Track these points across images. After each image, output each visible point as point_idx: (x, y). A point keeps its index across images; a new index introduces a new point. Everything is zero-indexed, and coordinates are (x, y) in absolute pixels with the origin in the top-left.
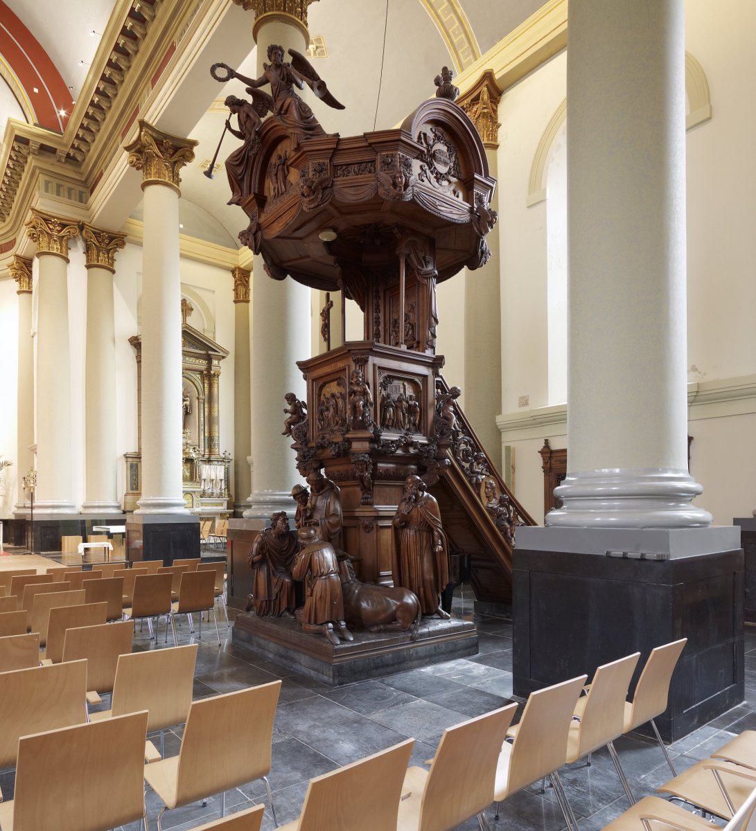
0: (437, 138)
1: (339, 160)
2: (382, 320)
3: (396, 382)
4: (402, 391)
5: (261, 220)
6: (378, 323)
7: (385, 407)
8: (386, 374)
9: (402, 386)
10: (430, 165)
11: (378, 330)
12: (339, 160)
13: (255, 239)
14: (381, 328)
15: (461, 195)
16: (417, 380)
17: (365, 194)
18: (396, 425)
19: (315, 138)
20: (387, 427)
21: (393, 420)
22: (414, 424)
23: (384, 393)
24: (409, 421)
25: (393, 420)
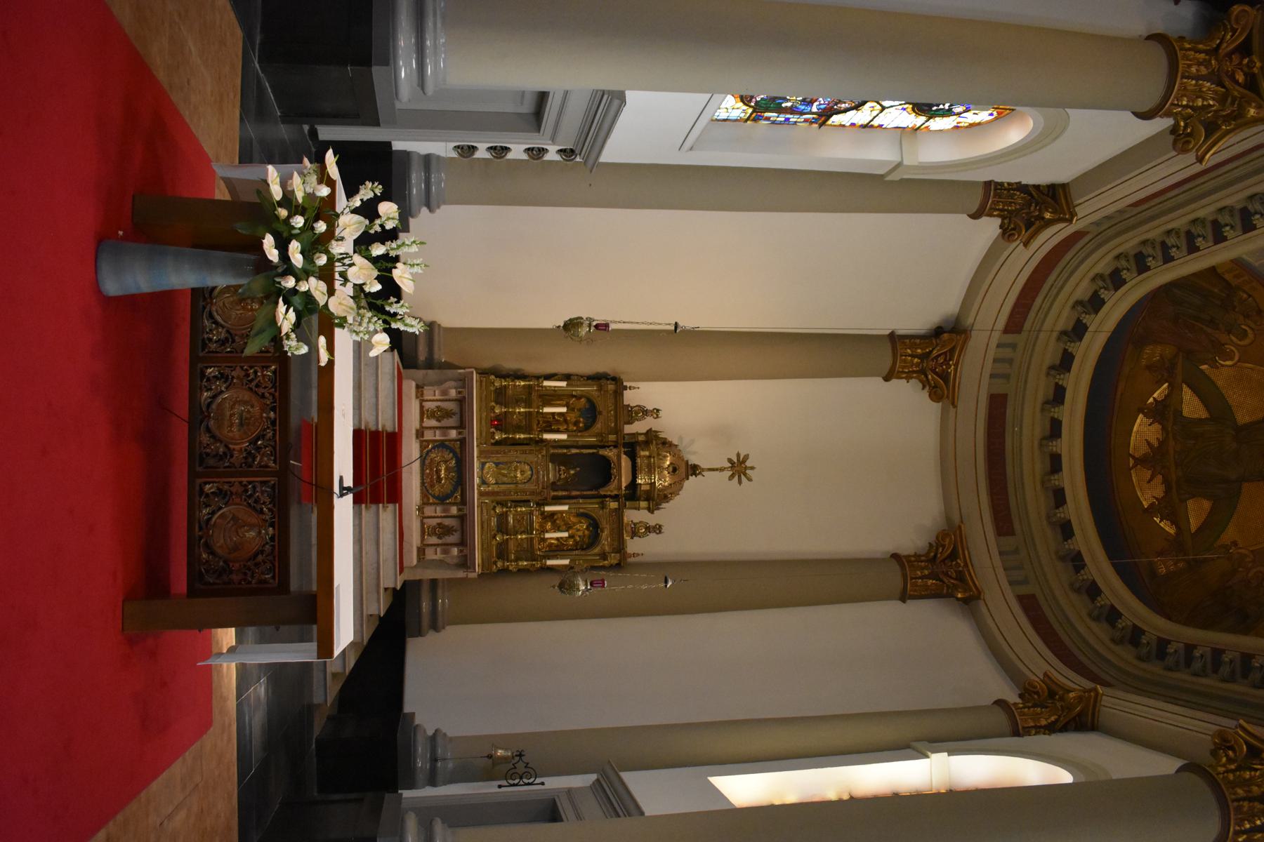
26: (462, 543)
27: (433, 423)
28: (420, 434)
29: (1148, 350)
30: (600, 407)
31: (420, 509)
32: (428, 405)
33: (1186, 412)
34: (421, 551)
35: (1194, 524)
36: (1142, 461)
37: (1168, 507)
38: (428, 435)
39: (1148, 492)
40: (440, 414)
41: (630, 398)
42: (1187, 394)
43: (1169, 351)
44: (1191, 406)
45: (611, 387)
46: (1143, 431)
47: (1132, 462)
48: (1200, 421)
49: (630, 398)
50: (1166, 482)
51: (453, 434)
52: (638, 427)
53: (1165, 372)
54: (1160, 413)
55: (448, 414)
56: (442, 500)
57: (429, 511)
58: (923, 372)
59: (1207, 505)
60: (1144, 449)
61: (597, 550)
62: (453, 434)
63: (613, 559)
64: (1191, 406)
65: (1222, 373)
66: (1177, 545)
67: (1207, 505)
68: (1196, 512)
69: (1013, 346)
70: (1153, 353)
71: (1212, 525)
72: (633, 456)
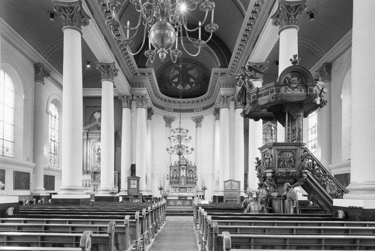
0: (293, 76)
1: (259, 93)
2: (290, 129)
3: (285, 153)
4: (287, 155)
5: (245, 109)
6: (289, 130)
7: (279, 161)
8: (280, 151)
9: (287, 154)
10: (289, 86)
11: (289, 133)
12: (259, 93)
13: (244, 114)
14: (290, 132)
15: (303, 91)
16: (293, 151)
17: (266, 102)
18: (284, 166)
19: (253, 89)
20: (280, 168)
21: (283, 165)
22: (292, 166)
23: (280, 157)
24: (290, 165)
25: (283, 165)
26: (192, 188)
27: (176, 191)
28: (178, 193)
29: (167, 87)
30: (174, 169)
31: (187, 193)
32: (174, 192)
33: (177, 81)
34: (193, 193)
35: (194, 81)
36: (184, 87)
37: (191, 84)
38: (178, 192)
39: (188, 87)
40: (175, 190)
41: (173, 165)
42: (174, 81)
43: (168, 84)
44: (176, 80)
45: (171, 168)
46: (180, 87)
47: (184, 89)
48: (178, 79)
49: (173, 165)
50: (187, 84)
51: (178, 188)
52: (177, 164)
53: (171, 84)
54: (177, 84)
55: (175, 190)
56: (186, 190)
57: (188, 192)
58: (170, 122)
59: (191, 79)
60: (182, 87)
61: (193, 170)
62: (178, 188)
63: (195, 168)
64: (176, 80)
65: (171, 76)
66: (196, 84)
67: (191, 79)
68: (192, 80)
69: (166, 108)
70: (168, 86)
71: (194, 78)
72: (181, 165)
